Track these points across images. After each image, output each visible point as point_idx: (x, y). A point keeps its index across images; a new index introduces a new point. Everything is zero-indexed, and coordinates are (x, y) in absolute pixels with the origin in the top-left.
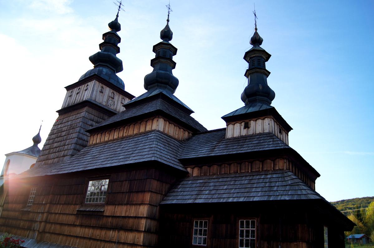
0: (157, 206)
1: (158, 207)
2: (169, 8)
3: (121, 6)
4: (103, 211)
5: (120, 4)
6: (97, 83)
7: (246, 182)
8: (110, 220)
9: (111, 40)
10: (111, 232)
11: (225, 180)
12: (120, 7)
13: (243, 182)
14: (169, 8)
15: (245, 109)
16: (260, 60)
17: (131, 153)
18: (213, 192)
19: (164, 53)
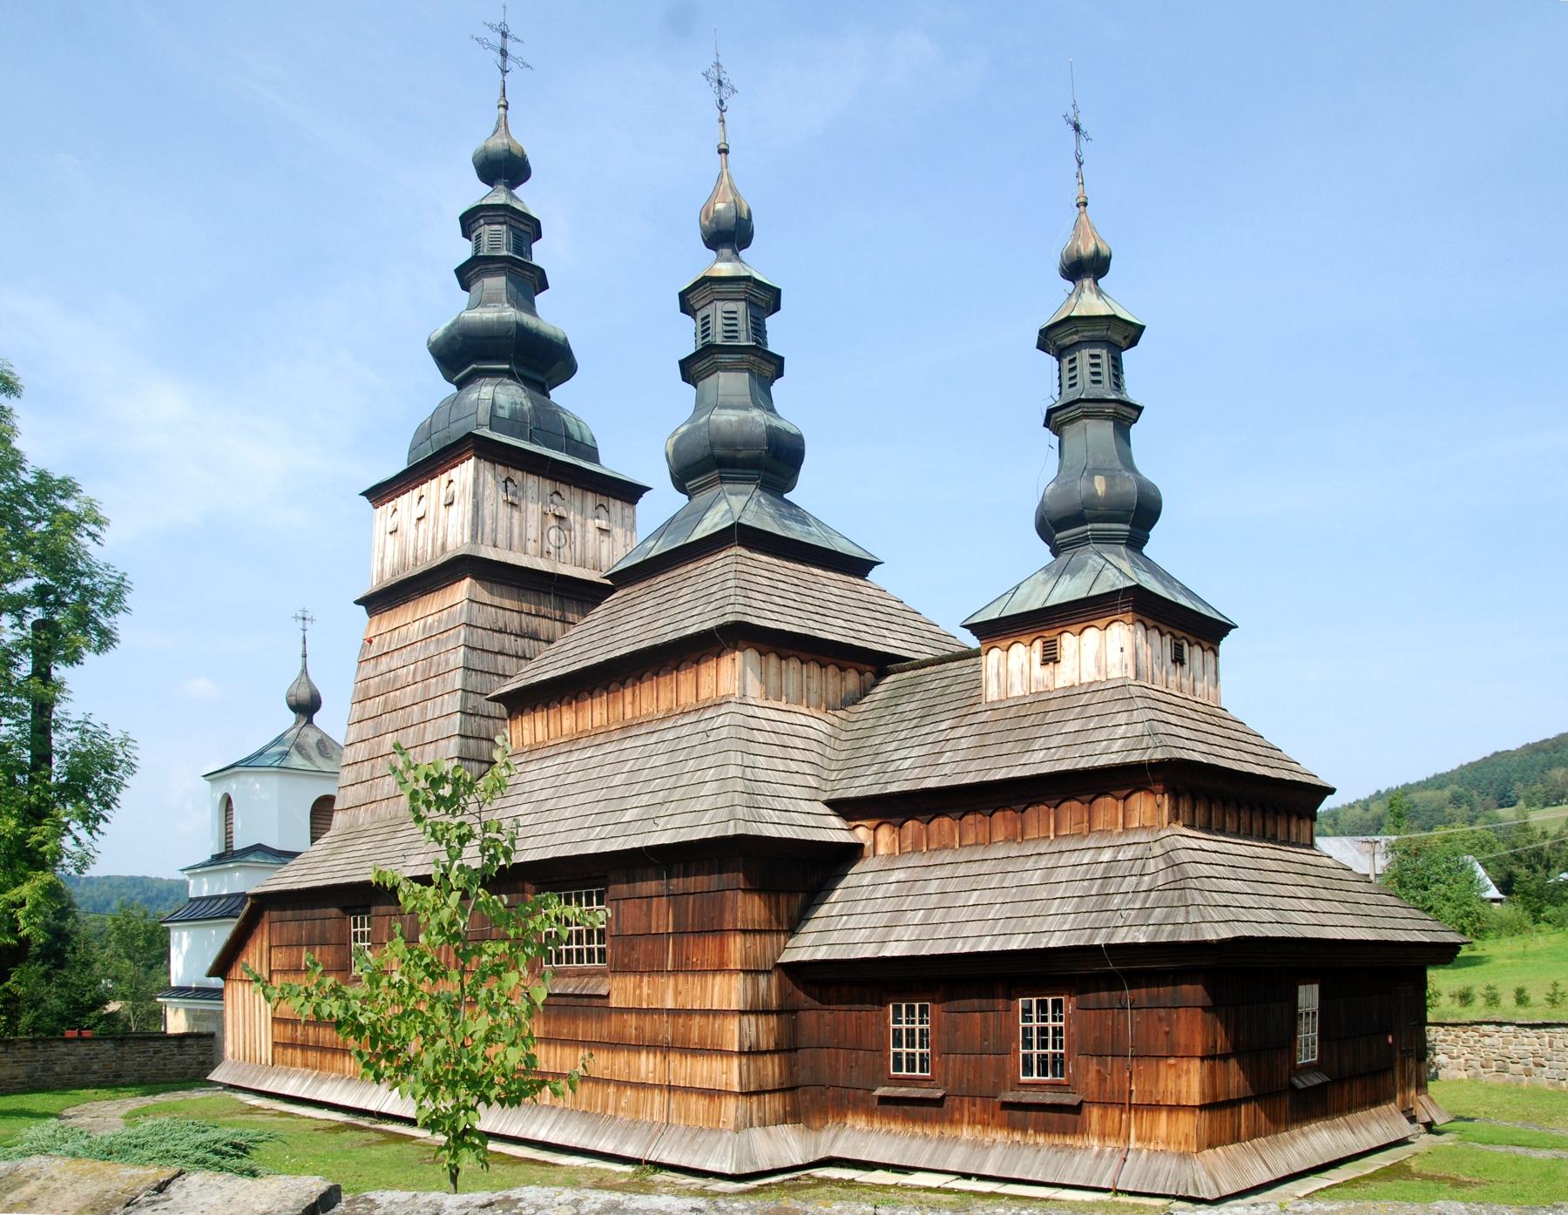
0: (768, 972)
1: (774, 979)
2: (720, 83)
3: (511, 46)
4: (604, 992)
5: (504, 35)
6: (485, 466)
7: (1037, 877)
8: (632, 1020)
9: (504, 247)
10: (644, 1055)
11: (974, 868)
12: (504, 53)
13: (1028, 878)
14: (720, 83)
15: (1046, 582)
16: (1098, 356)
17: (660, 797)
18: (937, 916)
19: (734, 330)
